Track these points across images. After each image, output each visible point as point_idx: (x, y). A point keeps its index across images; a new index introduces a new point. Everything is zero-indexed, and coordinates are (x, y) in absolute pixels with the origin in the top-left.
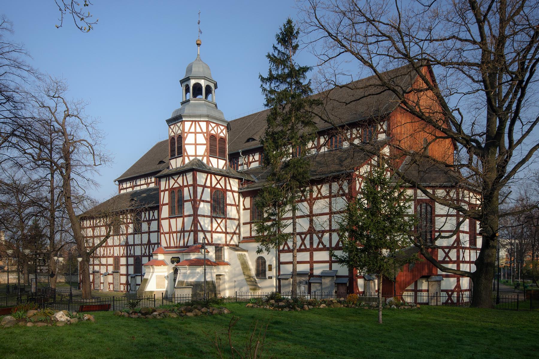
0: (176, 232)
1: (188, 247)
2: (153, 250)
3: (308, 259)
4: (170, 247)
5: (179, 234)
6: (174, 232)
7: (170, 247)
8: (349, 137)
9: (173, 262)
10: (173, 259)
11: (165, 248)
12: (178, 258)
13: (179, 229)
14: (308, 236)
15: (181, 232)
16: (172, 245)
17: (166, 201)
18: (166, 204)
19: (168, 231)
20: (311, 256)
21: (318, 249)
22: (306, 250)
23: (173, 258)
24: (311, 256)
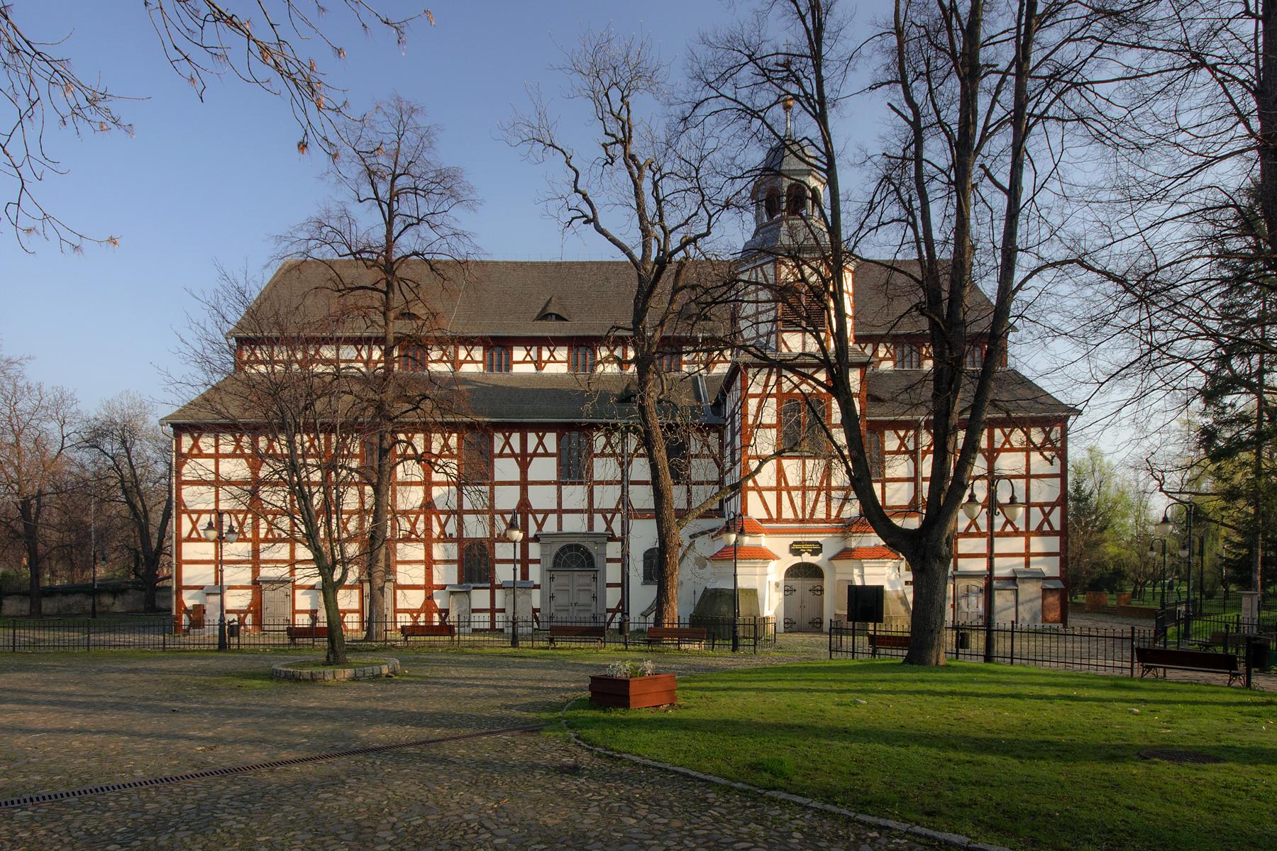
0: (804, 489)
1: (842, 521)
2: (540, 526)
3: (984, 550)
4: (779, 519)
5: (812, 495)
6: (796, 489)
7: (779, 519)
8: (365, 357)
9: (795, 551)
10: (797, 547)
11: (761, 521)
12: (817, 543)
13: (815, 480)
14: (422, 517)
15: (819, 490)
16: (787, 513)
17: (769, 416)
18: (770, 426)
19: (774, 484)
20: (991, 545)
21: (1003, 534)
22: (979, 534)
23: (795, 543)
24: (991, 545)
